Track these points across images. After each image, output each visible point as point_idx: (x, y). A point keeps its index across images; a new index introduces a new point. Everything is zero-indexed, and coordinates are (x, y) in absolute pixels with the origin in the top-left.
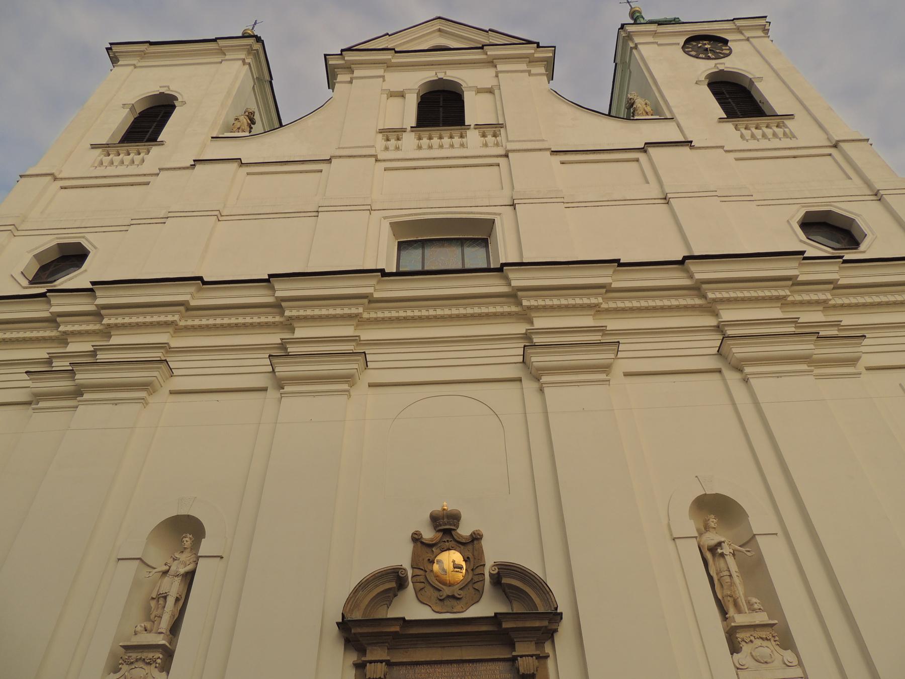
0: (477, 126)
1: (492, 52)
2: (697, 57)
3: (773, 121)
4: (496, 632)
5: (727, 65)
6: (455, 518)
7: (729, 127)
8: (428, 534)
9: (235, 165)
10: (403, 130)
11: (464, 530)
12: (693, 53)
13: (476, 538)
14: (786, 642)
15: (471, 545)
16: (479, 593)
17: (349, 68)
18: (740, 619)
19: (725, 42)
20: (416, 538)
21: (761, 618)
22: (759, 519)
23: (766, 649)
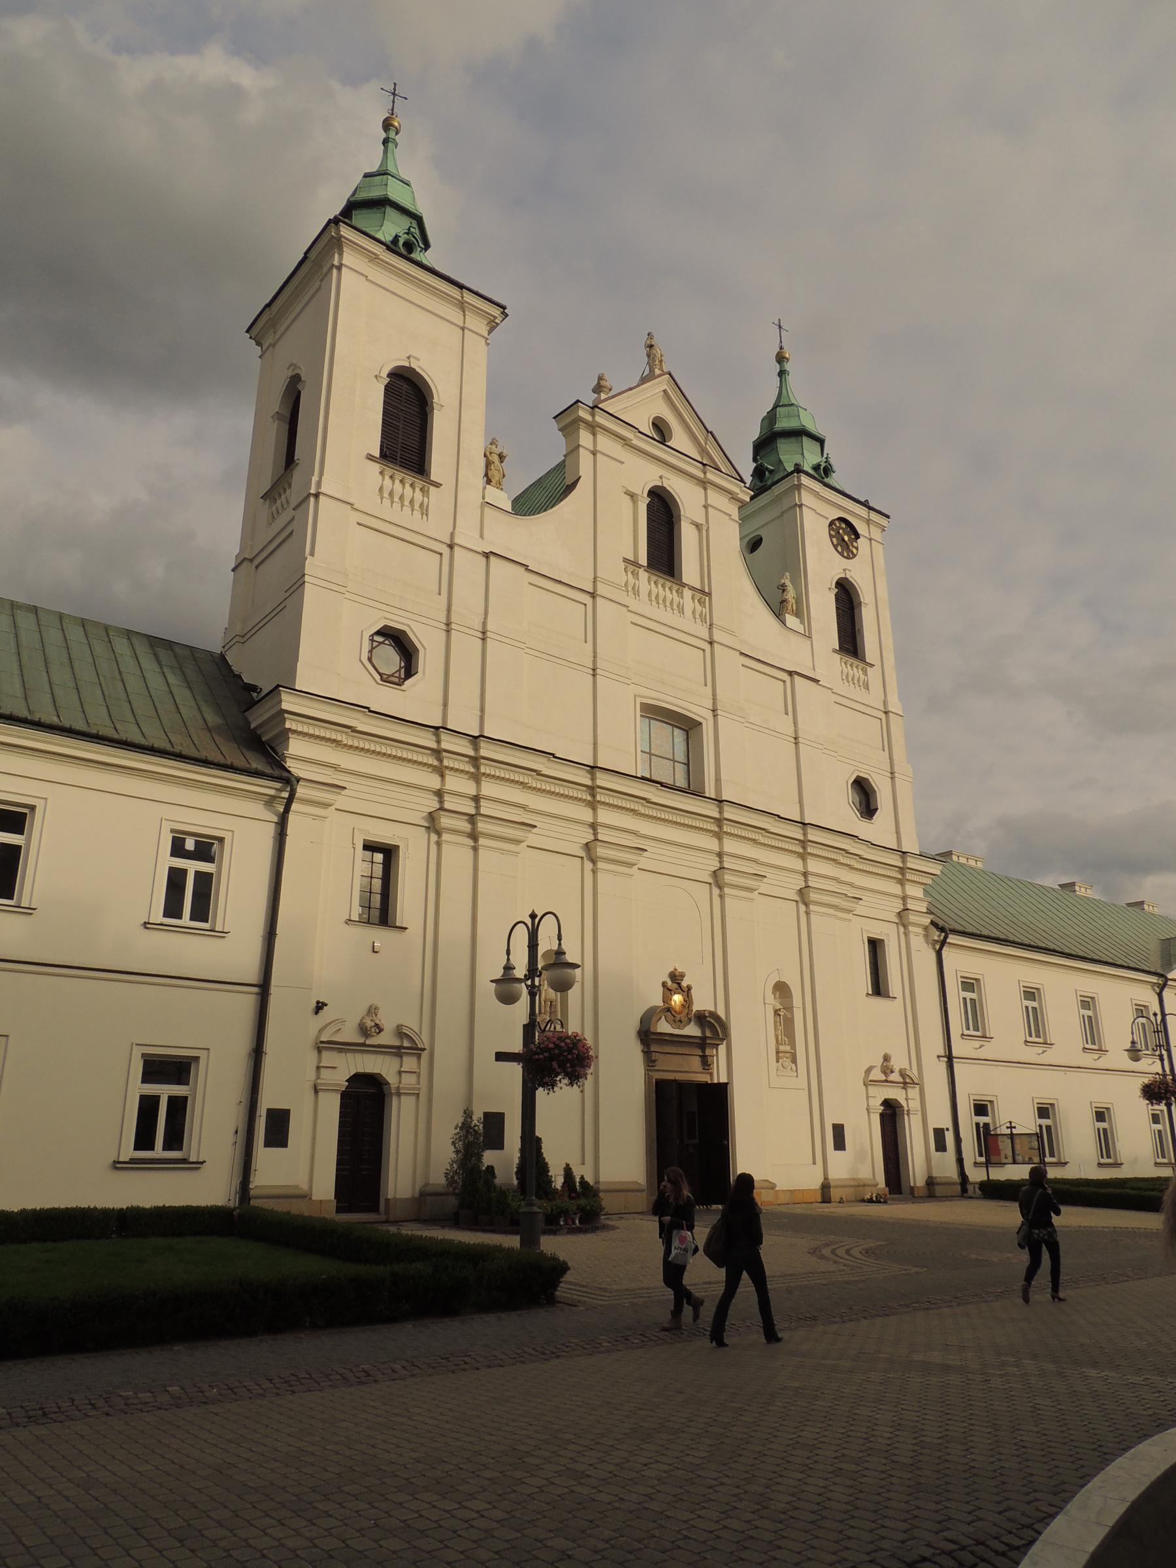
0: (692, 588)
1: (712, 476)
2: (835, 547)
3: (861, 665)
4: (702, 1044)
5: (852, 574)
6: (682, 976)
7: (837, 657)
8: (670, 983)
9: (522, 569)
10: (640, 566)
11: (684, 984)
12: (835, 540)
13: (689, 988)
14: (794, 1061)
15: (687, 992)
16: (690, 1020)
17: (593, 428)
18: (782, 1048)
19: (857, 536)
20: (664, 984)
21: (788, 1048)
22: (797, 1001)
23: (787, 1062)
